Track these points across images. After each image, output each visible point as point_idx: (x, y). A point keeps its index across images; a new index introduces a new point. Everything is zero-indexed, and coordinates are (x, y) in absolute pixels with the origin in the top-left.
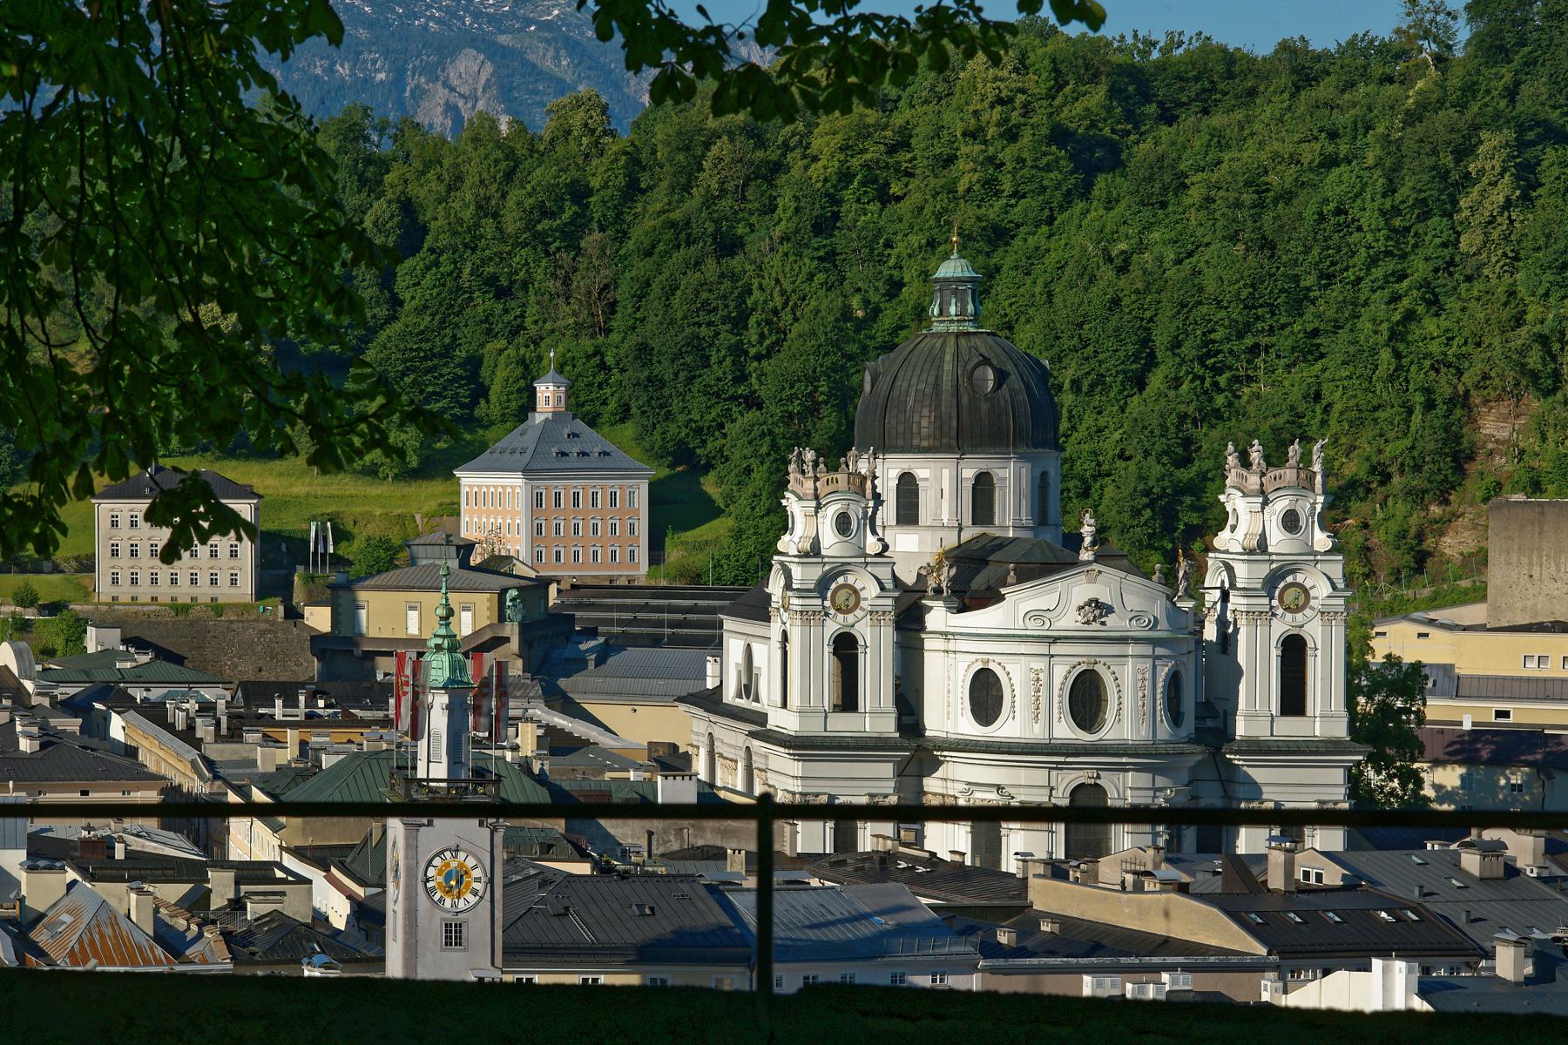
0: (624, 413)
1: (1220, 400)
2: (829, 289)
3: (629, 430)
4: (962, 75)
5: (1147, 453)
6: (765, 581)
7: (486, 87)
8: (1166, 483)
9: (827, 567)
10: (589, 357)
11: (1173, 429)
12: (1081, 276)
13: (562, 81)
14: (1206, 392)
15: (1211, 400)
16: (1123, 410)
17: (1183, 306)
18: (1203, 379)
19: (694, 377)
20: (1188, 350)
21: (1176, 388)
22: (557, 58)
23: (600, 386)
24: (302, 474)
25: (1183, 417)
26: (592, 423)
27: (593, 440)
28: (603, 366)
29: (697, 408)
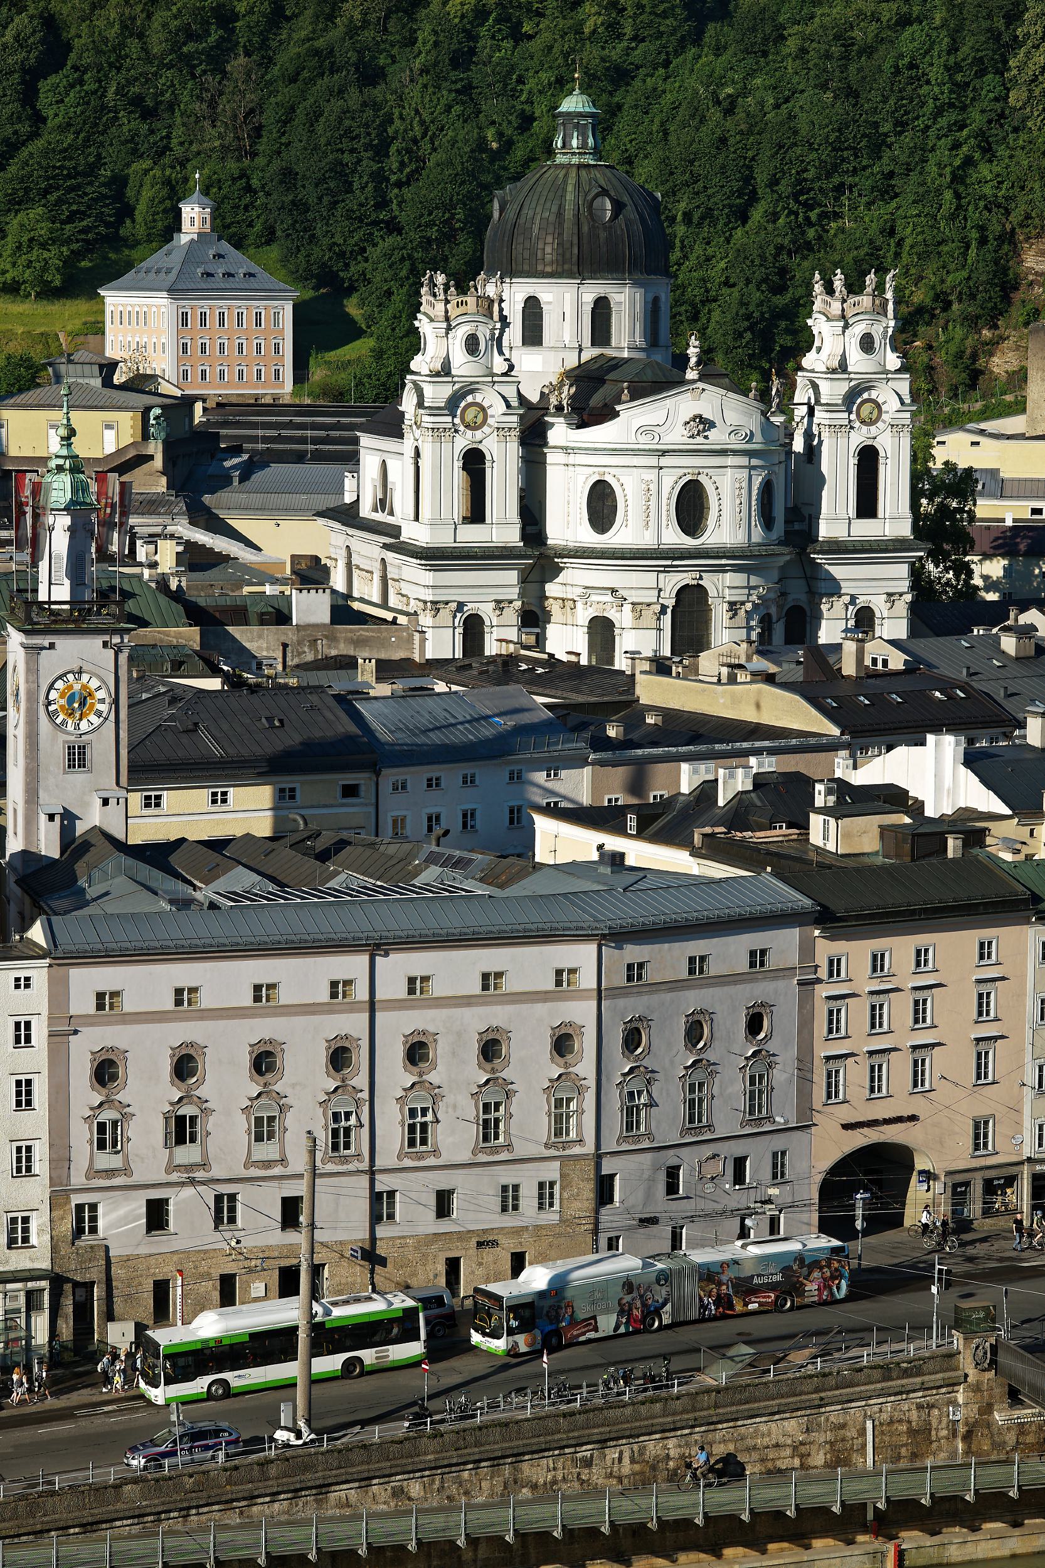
0: (269, 237)
1: (811, 233)
3: (274, 252)
5: (748, 281)
8: (765, 309)
9: (457, 386)
11: (770, 259)
14: (800, 226)
15: (803, 233)
16: (728, 241)
17: (781, 147)
18: (797, 214)
20: (784, 188)
21: (774, 222)
25: (780, 248)
26: (238, 244)
27: (239, 261)
28: (249, 189)
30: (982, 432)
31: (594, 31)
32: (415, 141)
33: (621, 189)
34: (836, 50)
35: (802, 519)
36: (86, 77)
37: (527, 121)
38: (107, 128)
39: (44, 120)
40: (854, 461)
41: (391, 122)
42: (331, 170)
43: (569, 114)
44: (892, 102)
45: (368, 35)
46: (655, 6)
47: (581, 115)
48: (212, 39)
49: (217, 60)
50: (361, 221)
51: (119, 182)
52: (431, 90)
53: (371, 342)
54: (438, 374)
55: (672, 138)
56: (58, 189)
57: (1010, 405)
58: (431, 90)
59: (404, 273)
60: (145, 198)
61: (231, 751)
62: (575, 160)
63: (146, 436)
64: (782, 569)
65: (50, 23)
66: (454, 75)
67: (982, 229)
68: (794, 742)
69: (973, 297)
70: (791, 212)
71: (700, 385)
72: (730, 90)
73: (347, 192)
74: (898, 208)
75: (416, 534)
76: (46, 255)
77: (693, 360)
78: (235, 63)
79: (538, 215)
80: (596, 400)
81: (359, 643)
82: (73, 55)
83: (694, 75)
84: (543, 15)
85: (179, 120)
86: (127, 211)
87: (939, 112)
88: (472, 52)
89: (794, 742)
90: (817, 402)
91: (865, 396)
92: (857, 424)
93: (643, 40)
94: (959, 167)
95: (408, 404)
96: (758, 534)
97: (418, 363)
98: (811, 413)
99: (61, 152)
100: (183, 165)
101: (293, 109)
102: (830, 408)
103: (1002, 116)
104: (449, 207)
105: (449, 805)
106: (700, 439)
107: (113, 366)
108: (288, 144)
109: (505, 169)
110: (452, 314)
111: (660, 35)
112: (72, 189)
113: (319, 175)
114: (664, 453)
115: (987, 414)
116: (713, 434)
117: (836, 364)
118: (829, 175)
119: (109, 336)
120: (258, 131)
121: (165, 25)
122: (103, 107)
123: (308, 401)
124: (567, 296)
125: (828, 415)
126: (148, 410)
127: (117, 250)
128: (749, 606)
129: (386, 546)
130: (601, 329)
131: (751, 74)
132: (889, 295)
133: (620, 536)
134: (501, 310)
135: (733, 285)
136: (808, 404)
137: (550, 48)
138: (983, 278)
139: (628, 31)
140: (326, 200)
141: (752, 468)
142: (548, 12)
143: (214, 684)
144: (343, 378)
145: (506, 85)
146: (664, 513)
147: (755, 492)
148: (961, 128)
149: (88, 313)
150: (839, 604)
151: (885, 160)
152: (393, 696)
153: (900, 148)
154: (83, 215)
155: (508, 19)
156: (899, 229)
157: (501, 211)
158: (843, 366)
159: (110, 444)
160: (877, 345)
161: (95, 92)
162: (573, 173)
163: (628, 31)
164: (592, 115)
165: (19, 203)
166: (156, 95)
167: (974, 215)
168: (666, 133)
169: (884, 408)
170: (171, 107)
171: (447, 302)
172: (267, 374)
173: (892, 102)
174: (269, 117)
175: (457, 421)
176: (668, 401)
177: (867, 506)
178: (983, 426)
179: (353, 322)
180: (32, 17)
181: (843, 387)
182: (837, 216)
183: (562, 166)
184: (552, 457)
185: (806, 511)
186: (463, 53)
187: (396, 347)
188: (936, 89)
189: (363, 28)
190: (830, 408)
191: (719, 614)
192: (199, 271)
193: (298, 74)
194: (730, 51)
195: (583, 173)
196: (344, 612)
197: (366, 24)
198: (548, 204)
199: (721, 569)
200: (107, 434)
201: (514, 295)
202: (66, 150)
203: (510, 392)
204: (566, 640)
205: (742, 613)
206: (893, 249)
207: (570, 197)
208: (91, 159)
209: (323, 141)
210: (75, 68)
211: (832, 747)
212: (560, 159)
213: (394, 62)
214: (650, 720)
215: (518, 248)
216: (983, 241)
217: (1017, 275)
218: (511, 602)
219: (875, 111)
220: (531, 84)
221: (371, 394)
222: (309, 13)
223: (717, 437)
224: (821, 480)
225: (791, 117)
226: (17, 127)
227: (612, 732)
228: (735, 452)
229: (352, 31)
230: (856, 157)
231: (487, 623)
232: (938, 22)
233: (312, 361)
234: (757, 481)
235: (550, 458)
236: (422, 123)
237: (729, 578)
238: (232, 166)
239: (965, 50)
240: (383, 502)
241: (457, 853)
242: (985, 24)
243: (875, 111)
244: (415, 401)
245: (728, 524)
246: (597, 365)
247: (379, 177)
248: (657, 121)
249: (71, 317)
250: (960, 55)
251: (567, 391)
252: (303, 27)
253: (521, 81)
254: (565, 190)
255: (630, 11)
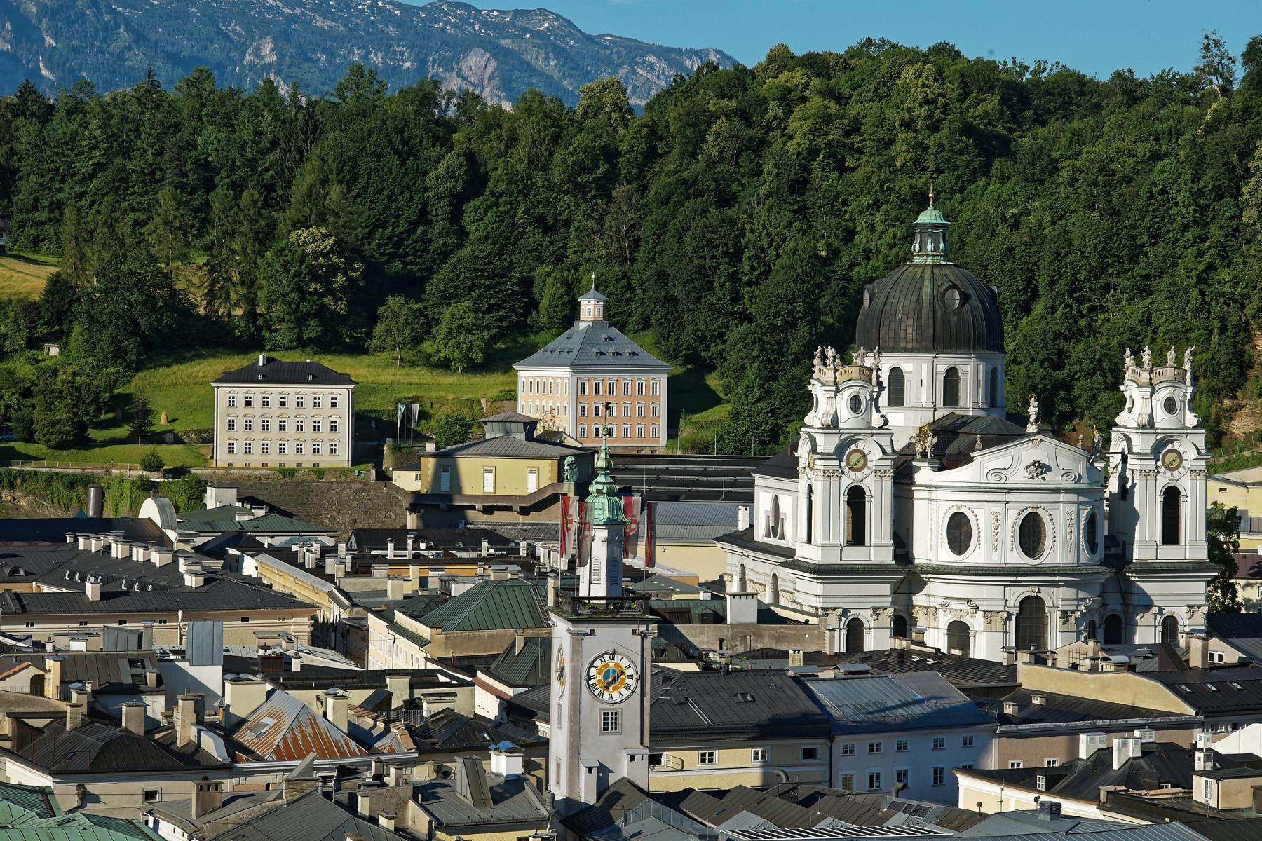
0: (645, 324)
1: (1083, 323)
2: (804, 234)
3: (649, 336)
4: (897, 82)
5: (1033, 360)
6: (795, 448)
7: (491, 78)
10: (618, 280)
11: (1051, 342)
12: (986, 231)
13: (551, 77)
14: (1073, 317)
15: (1076, 322)
16: (1015, 328)
18: (1071, 308)
19: (701, 297)
20: (1061, 286)
21: (1053, 313)
22: (547, 59)
23: (627, 302)
24: (387, 366)
25: (1058, 335)
26: (621, 329)
27: (625, 343)
28: (629, 287)
29: (702, 321)
30: (1227, 481)
31: (903, 166)
32: (763, 250)
33: (966, 283)
34: (1101, 179)
35: (1117, 545)
36: (501, 201)
37: (850, 234)
38: (517, 239)
39: (467, 234)
40: (1160, 499)
41: (743, 235)
42: (697, 272)
43: (925, 225)
44: (1148, 219)
45: (724, 168)
46: (952, 145)
47: (935, 226)
48: (600, 171)
49: (604, 188)
50: (719, 312)
51: (527, 282)
52: (775, 210)
53: (729, 407)
54: (828, 427)
55: (969, 248)
56: (480, 286)
57: (1248, 460)
58: (775, 210)
59: (755, 352)
60: (548, 294)
61: (716, 720)
62: (930, 261)
63: (561, 479)
64: (1103, 584)
65: (471, 158)
66: (791, 199)
67: (1222, 319)
68: (1159, 719)
69: (1215, 373)
70: (1067, 306)
71: (1039, 437)
72: (1014, 211)
73: (708, 290)
74: (1153, 303)
75: (808, 553)
76: (471, 338)
77: (1033, 417)
78: (620, 190)
79: (901, 304)
80: (951, 449)
81: (779, 638)
82: (491, 184)
83: (985, 198)
84: (863, 153)
85: (573, 234)
86: (533, 305)
87: (1185, 228)
88: (806, 181)
89: (1159, 719)
90: (1130, 451)
91: (1169, 447)
92: (1162, 470)
93: (943, 172)
94: (1203, 272)
95: (803, 452)
96: (1085, 556)
97: (812, 418)
98: (1124, 460)
99: (482, 258)
100: (576, 270)
101: (665, 225)
102: (1141, 456)
103: (1237, 231)
104: (791, 300)
105: (887, 763)
106: (1038, 480)
107: (530, 425)
108: (660, 253)
109: (834, 272)
110: (840, 380)
111: (958, 167)
112: (489, 288)
113: (686, 276)
114: (1010, 491)
115: (1228, 467)
116: (1048, 476)
117: (1145, 421)
118: (1096, 277)
119: (521, 402)
120: (637, 242)
121: (564, 161)
122: (514, 224)
123: (679, 453)
124: (925, 367)
125: (1139, 462)
126: (563, 458)
127: (525, 335)
128: (1078, 614)
129: (782, 564)
130: (951, 396)
131: (1031, 198)
132: (1187, 367)
133: (977, 555)
134: (878, 377)
135: (1020, 363)
136: (1122, 453)
137: (870, 177)
138: (1224, 358)
139: (931, 164)
140: (692, 295)
141: (1079, 503)
142: (866, 150)
143: (692, 667)
144: (707, 435)
145: (833, 206)
146: (1009, 539)
147: (1082, 523)
148: (1204, 240)
149: (504, 384)
150: (1149, 616)
151: (1142, 265)
152: (835, 679)
153: (1155, 255)
154: (500, 307)
155: (835, 156)
156: (1154, 319)
157: (871, 300)
158: (1151, 423)
159: (532, 485)
160: (1178, 407)
161: (508, 213)
162: (929, 271)
163: (931, 164)
164: (943, 226)
165: (450, 298)
166: (556, 214)
167: (1216, 309)
168: (963, 244)
169: (1184, 456)
170: (567, 224)
171: (836, 370)
172: (647, 431)
173: (1148, 219)
174: (645, 231)
175: (843, 464)
176: (1012, 449)
177: (1171, 535)
178: (1227, 476)
179: (713, 392)
180: (458, 155)
181: (1152, 440)
182: (1103, 309)
183: (919, 265)
184: (918, 494)
185: (1120, 539)
186: (799, 182)
187: (749, 411)
188: (1183, 210)
189: (719, 162)
190: (1141, 456)
191: (1054, 620)
192: (595, 350)
193: (669, 198)
194: (1014, 180)
195: (937, 270)
196: (767, 616)
197: (722, 159)
198: (909, 295)
199: (1056, 585)
200: (532, 477)
201: (887, 363)
202: (486, 257)
203: (885, 441)
204: (937, 639)
205: (1072, 620)
206: (1150, 336)
207: (926, 289)
208: (506, 264)
209: (690, 249)
210: (492, 194)
211: (1188, 725)
212: (917, 260)
213: (744, 189)
214: (1036, 701)
215: (884, 329)
216: (1223, 329)
217: (1251, 357)
218: (885, 609)
219: (1134, 227)
220: (854, 205)
221: (731, 447)
222: (676, 151)
223: (1052, 478)
224: (1135, 516)
225: (1066, 232)
226: (446, 239)
227: (1008, 710)
228: (1067, 491)
229: (711, 165)
230: (1119, 263)
231: (866, 625)
232: (1182, 157)
233: (682, 422)
234: (1084, 514)
235: (917, 494)
236: (769, 235)
237: (1062, 592)
238: (616, 269)
239: (1205, 179)
240: (775, 530)
241: (915, 803)
242: (1222, 159)
243: (1134, 227)
244: (809, 447)
245: (1061, 548)
246: (948, 423)
247: (734, 278)
248: (955, 234)
249: (491, 386)
250: (1202, 183)
251: (931, 441)
252: (672, 162)
253: (845, 203)
254: (922, 284)
255: (932, 150)
